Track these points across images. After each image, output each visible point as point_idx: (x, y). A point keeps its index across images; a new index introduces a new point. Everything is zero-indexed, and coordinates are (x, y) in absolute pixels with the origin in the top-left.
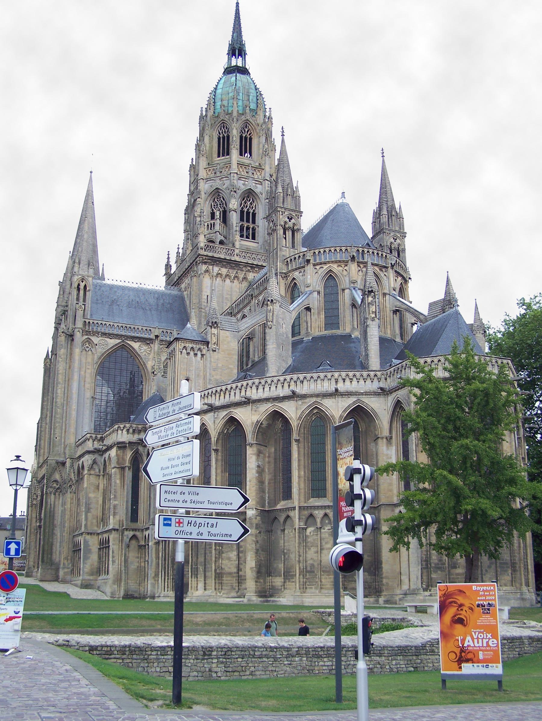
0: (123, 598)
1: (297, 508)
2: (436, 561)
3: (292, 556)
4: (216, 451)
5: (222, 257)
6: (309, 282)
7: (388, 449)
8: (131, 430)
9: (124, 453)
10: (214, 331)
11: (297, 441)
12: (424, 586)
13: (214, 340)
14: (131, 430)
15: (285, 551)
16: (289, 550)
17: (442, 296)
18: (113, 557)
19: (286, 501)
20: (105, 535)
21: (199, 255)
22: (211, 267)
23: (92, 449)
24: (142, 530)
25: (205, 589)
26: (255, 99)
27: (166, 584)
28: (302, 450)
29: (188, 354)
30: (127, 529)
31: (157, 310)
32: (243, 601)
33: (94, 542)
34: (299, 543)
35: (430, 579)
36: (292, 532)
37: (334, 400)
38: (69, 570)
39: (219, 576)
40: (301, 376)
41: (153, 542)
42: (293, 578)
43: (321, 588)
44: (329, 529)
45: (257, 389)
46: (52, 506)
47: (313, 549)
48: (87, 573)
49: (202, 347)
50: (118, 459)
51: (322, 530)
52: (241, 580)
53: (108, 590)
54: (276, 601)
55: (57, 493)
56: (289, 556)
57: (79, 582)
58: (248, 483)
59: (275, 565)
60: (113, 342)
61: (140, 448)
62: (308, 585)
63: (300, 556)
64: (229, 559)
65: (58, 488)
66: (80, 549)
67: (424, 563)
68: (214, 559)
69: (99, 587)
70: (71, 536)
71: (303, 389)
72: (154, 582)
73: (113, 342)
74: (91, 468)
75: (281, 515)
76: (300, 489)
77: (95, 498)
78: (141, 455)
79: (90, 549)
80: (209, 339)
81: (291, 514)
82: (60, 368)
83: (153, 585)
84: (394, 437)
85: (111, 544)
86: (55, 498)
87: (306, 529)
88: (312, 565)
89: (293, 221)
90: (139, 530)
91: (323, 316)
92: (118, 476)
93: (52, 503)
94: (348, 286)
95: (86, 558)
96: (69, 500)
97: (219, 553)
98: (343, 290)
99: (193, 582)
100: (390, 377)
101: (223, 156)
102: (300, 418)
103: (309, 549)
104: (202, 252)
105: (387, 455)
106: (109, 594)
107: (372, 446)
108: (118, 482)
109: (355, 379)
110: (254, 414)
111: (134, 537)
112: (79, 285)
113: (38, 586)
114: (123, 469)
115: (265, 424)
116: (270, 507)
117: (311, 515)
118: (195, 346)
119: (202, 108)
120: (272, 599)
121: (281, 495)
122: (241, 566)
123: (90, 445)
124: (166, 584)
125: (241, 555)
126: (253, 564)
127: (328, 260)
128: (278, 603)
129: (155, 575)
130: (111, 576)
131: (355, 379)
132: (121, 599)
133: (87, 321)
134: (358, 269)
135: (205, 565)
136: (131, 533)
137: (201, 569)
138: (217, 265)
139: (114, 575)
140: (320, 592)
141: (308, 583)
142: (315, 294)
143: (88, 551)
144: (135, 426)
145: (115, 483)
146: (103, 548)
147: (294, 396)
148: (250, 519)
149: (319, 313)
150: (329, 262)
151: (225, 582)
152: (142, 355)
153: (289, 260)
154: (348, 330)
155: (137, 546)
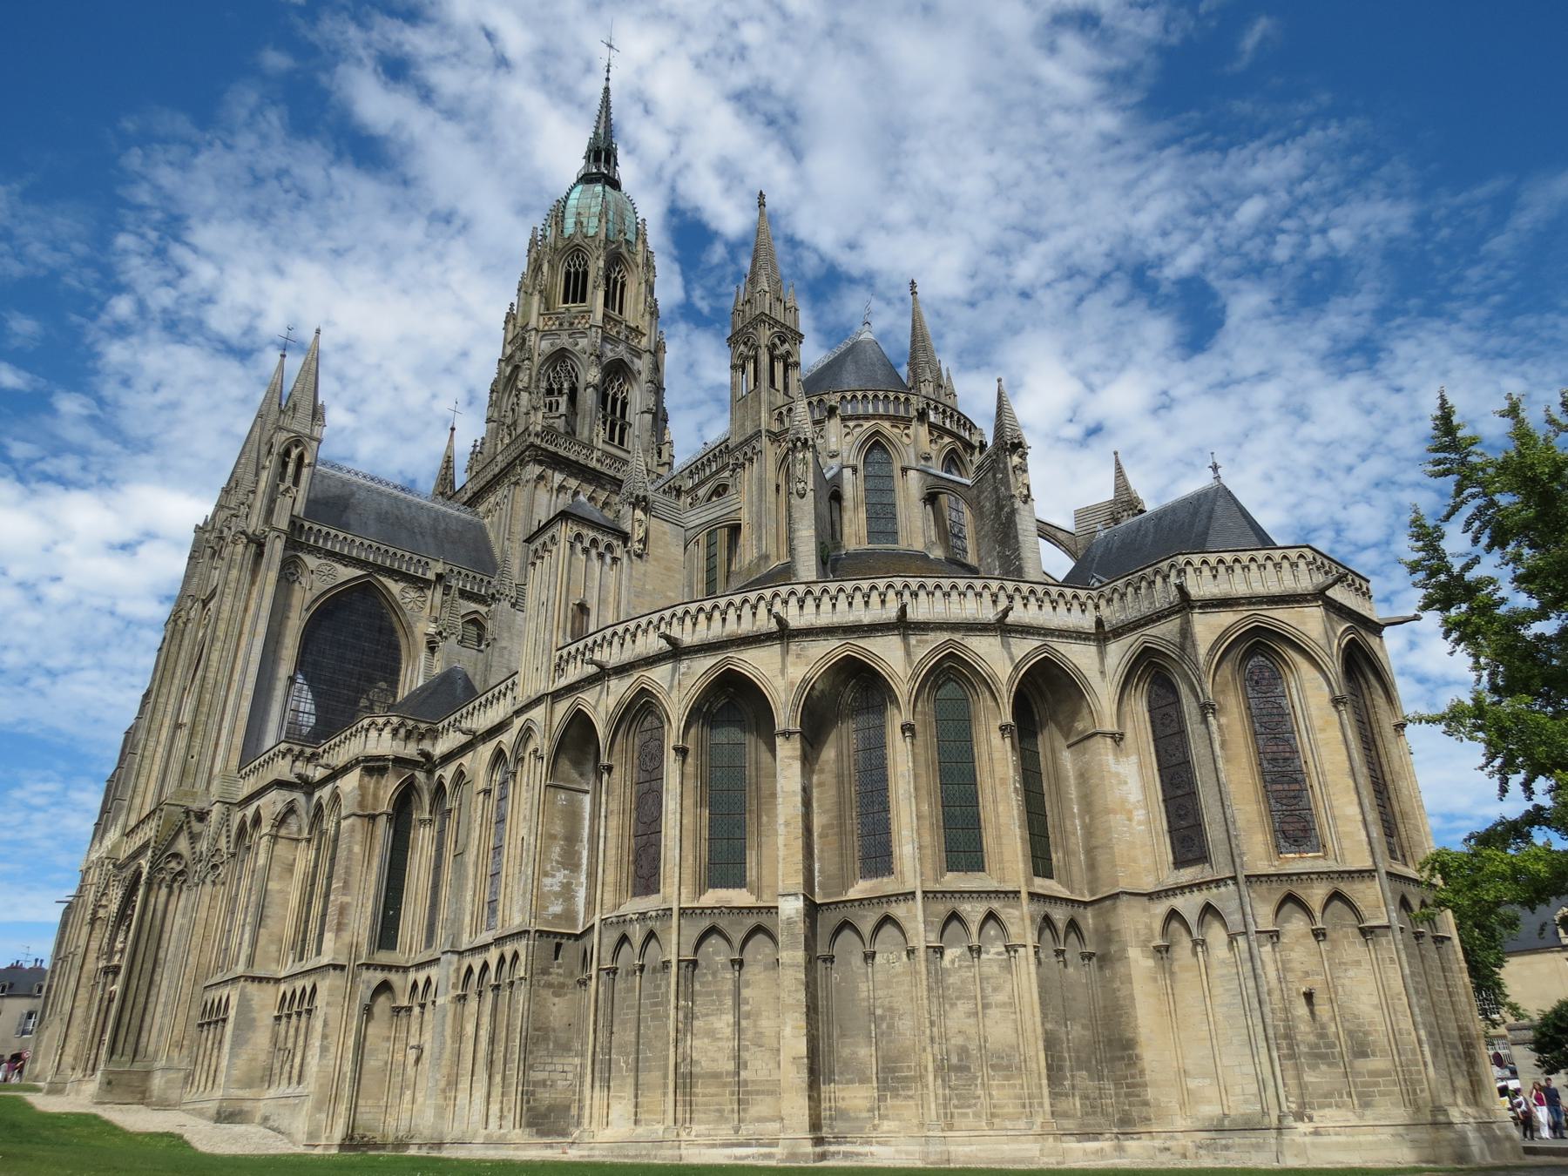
0: (342, 1146)
1: (919, 895)
2: (1312, 1038)
3: (905, 1025)
4: (682, 752)
5: (573, 457)
6: (833, 447)
7: (1117, 762)
8: (402, 731)
9: (378, 782)
10: (639, 514)
11: (907, 729)
12: (1293, 1106)
13: (639, 533)
14: (402, 731)
15: (879, 1012)
16: (891, 1009)
17: (1110, 495)
18: (324, 1037)
19: (874, 881)
20: (299, 984)
21: (532, 445)
22: (550, 472)
23: (292, 778)
24: (406, 969)
25: (636, 1122)
26: (633, 228)
27: (495, 1108)
28: (920, 750)
29: (586, 551)
30: (368, 966)
31: (435, 536)
32: (770, 1156)
33: (265, 1000)
34: (930, 989)
35: (1302, 1086)
36: (899, 958)
37: (991, 639)
38: (182, 1074)
39: (685, 1082)
40: (914, 583)
41: (449, 998)
42: (909, 1088)
43: (993, 1115)
44: (999, 954)
45: (801, 607)
46: (159, 914)
47: (963, 1007)
48: (238, 1081)
49: (615, 543)
50: (363, 796)
51: (983, 956)
52: (747, 1093)
53: (300, 1125)
54: (858, 1154)
55: (176, 885)
56: (891, 1026)
57: (212, 1107)
58: (781, 830)
59: (846, 1052)
60: (346, 573)
61: (420, 776)
62: (956, 1107)
63: (932, 1024)
64: (711, 1034)
65: (181, 873)
66: (224, 1020)
67: (1284, 1043)
68: (672, 1034)
69: (266, 1119)
70: (199, 989)
71: (920, 610)
72: (441, 1102)
73: (346, 573)
74: (281, 821)
75: (865, 917)
76: (920, 848)
77: (280, 891)
78: (419, 792)
79: (254, 1020)
80: (628, 530)
81: (898, 911)
82: (226, 608)
83: (440, 1112)
84: (1129, 735)
85: (320, 1000)
86: (170, 893)
87: (940, 951)
88: (963, 1051)
89: (786, 346)
90: (397, 968)
91: (863, 515)
92: (358, 837)
93: (160, 907)
94: (913, 464)
95: (238, 1041)
96: (207, 899)
97: (686, 1017)
98: (904, 470)
99: (596, 1102)
100: (1110, 601)
101: (574, 301)
102: (914, 676)
103: (953, 1005)
104: (538, 441)
105: (1118, 775)
106: (301, 1137)
107: (1067, 758)
108: (357, 849)
109: (1032, 600)
110: (795, 664)
111: (385, 987)
112: (287, 453)
113: (96, 1117)
114: (373, 818)
115: (816, 693)
116: (825, 895)
117: (954, 916)
118: (600, 537)
119: (535, 228)
120: (842, 1148)
121: (858, 865)
122: (745, 1055)
123: (283, 769)
124: (495, 1108)
125: (744, 1023)
126: (802, 1047)
127: (871, 411)
128: (867, 1163)
129: (449, 1083)
130: (311, 1085)
131: (1032, 600)
132: (334, 1151)
133: (298, 522)
134: (928, 438)
135: (638, 1052)
136: (379, 977)
137: (622, 1062)
138: (561, 471)
139: (321, 1086)
140: (991, 1124)
141: (955, 1102)
142: (847, 473)
143: (246, 1023)
144: (411, 723)
145: (350, 851)
146: (289, 1016)
147: (903, 626)
148: (790, 922)
149: (856, 508)
150: (873, 417)
151: (700, 1099)
152: (407, 608)
153: (784, 410)
154: (918, 546)
155: (388, 1012)
